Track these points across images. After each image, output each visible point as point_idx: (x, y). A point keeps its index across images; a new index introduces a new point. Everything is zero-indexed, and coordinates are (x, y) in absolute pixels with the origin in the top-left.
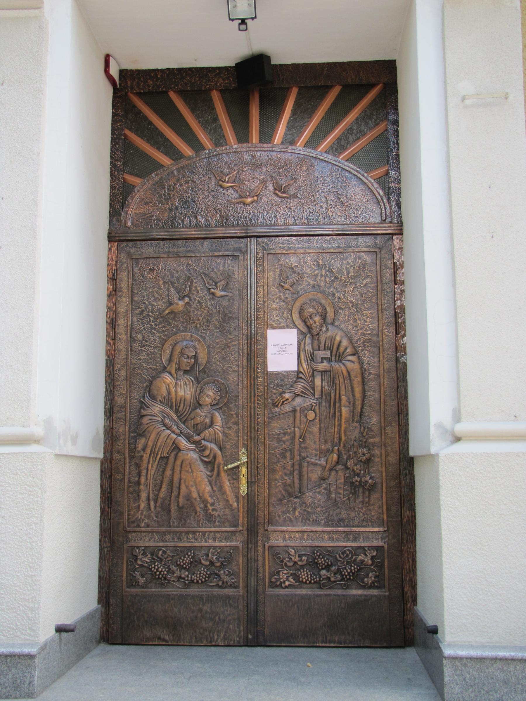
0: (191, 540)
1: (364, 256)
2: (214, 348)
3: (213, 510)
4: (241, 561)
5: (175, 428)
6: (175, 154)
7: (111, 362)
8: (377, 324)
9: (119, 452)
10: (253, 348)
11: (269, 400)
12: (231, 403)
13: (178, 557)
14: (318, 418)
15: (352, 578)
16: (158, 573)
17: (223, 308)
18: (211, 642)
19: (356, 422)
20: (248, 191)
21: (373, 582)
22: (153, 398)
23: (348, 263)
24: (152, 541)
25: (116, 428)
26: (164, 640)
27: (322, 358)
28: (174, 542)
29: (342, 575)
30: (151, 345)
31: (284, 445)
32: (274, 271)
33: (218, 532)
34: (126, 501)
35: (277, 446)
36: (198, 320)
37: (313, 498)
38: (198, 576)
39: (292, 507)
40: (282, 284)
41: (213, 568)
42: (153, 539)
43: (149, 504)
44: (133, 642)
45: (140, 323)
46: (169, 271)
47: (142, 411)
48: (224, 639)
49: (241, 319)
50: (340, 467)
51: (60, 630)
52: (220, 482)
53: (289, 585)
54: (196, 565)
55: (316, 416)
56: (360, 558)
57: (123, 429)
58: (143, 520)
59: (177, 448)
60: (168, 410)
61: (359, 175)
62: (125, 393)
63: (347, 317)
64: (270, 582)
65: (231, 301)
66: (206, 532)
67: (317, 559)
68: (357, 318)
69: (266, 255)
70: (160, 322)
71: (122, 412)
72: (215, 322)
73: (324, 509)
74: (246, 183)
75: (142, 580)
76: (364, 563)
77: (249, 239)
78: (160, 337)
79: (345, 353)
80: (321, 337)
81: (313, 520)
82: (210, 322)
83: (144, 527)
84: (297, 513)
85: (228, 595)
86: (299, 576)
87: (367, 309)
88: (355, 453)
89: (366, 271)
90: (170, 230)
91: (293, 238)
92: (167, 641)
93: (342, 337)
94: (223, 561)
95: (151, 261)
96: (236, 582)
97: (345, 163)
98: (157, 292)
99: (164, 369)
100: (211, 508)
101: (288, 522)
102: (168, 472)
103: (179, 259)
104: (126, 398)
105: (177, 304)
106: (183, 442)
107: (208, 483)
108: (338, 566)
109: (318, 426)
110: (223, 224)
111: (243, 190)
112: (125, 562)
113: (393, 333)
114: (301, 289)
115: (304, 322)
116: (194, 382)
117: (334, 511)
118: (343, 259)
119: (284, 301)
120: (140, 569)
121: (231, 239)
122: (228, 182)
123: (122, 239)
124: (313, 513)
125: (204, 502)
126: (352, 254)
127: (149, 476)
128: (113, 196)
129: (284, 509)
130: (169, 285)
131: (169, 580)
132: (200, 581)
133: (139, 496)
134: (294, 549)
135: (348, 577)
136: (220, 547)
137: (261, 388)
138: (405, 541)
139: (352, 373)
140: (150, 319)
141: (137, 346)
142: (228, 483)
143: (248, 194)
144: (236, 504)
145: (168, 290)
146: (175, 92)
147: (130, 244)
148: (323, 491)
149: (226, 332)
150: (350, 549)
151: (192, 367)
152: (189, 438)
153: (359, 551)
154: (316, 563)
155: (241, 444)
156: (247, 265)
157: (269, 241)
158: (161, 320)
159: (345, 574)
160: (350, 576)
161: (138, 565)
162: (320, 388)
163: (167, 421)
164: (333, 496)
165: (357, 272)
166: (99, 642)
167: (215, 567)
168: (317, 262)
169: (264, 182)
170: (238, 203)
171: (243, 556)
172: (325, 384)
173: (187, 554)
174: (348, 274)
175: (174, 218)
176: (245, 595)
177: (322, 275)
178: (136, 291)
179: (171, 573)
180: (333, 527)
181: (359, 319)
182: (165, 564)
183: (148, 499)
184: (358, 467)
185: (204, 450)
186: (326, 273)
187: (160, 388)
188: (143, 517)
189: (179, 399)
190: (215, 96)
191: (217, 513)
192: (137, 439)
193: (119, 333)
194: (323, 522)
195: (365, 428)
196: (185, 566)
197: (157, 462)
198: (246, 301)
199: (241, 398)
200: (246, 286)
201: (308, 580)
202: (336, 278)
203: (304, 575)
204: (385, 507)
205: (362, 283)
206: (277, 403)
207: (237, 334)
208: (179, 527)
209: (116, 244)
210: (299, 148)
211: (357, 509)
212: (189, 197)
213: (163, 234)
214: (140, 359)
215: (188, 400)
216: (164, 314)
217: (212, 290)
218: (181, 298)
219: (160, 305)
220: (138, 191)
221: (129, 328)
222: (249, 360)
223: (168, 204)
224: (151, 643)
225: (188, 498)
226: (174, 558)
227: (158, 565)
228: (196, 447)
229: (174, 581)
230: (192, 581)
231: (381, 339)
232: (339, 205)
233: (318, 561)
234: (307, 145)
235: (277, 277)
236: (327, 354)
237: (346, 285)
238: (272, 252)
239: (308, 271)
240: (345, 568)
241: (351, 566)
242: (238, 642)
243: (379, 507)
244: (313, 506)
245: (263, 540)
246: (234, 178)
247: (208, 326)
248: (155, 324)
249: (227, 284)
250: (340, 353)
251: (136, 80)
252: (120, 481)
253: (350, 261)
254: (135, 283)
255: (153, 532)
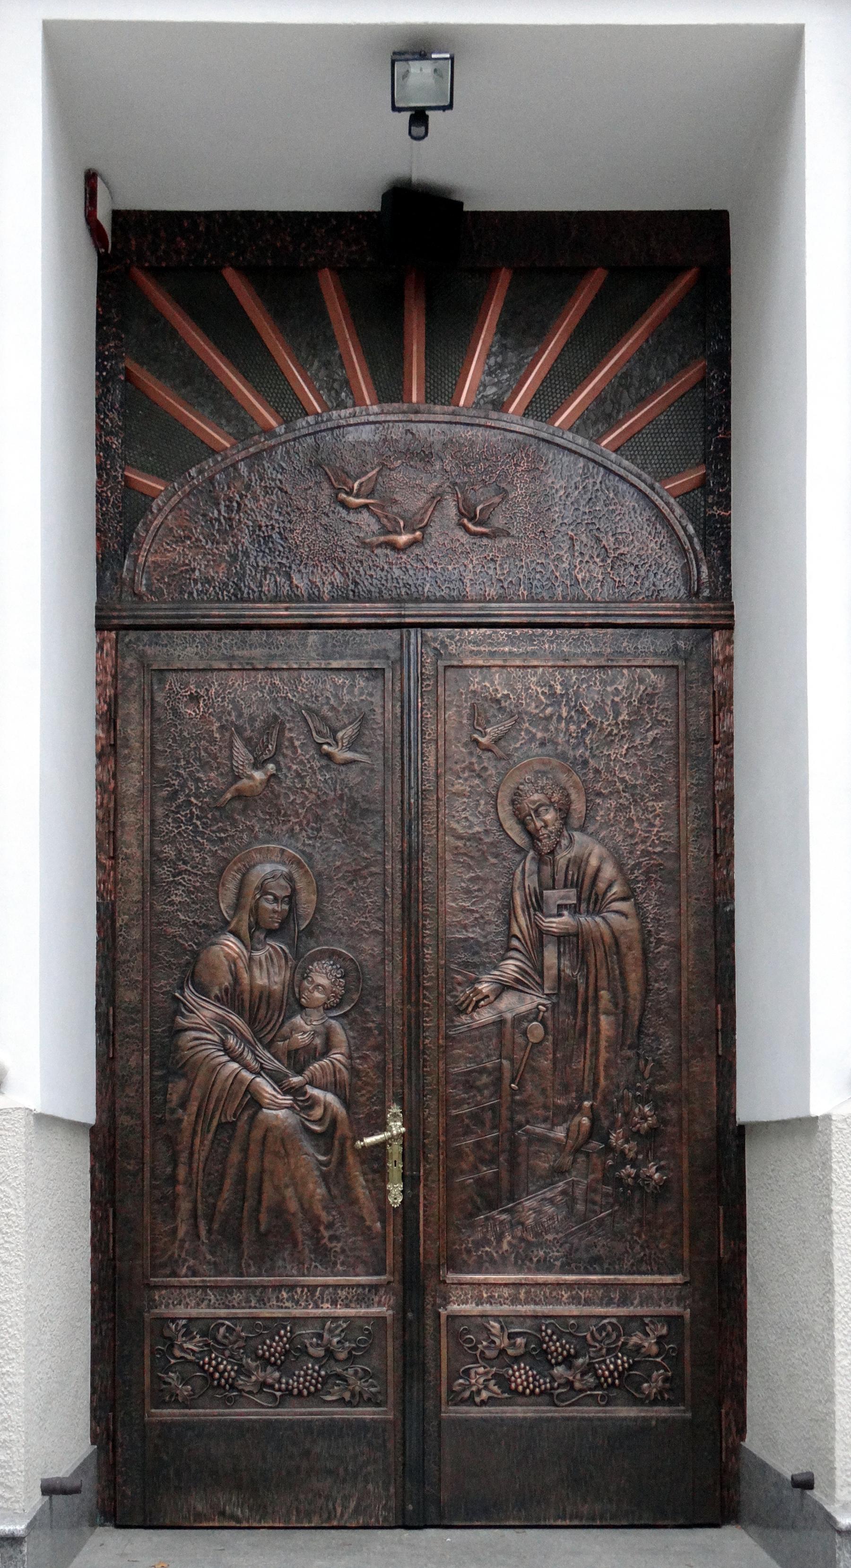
0: (287, 1304)
1: (652, 677)
2: (330, 879)
3: (332, 1238)
4: (390, 1349)
5: (249, 1057)
6: (242, 426)
7: (107, 907)
8: (676, 830)
9: (129, 1111)
10: (414, 881)
11: (449, 998)
12: (368, 1003)
13: (259, 1340)
14: (550, 1038)
15: (617, 1382)
16: (217, 1375)
17: (350, 789)
18: (329, 1519)
19: (630, 1047)
20: (402, 518)
21: (660, 1392)
22: (203, 990)
23: (617, 692)
24: (203, 1305)
25: (122, 1058)
26: (233, 1517)
27: (560, 907)
28: (250, 1307)
29: (598, 1377)
30: (195, 871)
31: (479, 1098)
32: (458, 706)
33: (342, 1287)
34: (147, 1218)
35: (464, 1099)
36: (297, 815)
37: (538, 1212)
38: (301, 1379)
39: (495, 1231)
40: (476, 736)
41: (332, 1362)
42: (206, 1302)
43: (196, 1226)
44: (168, 1522)
45: (170, 820)
46: (232, 701)
47: (179, 1019)
48: (356, 1512)
49: (388, 814)
50: (595, 1145)
51: (49, 1489)
52: (345, 1178)
53: (489, 1398)
54: (297, 1358)
55: (546, 1033)
56: (634, 1340)
57: (135, 1059)
58: (185, 1260)
59: (254, 1102)
60: (235, 1019)
61: (643, 486)
62: (140, 979)
63: (612, 815)
64: (450, 1391)
65: (367, 773)
66: (317, 1286)
67: (547, 1343)
68: (634, 818)
69: (441, 669)
70: (215, 819)
71: (134, 1021)
72: (332, 820)
73: (561, 1235)
74: (398, 497)
75: (185, 1390)
76: (643, 1350)
77: (405, 630)
78: (214, 854)
79: (609, 894)
80: (558, 857)
81: (539, 1261)
82: (322, 821)
83: (186, 1276)
84: (505, 1246)
85: (364, 1420)
86: (509, 1380)
87: (657, 797)
88: (626, 1115)
89: (655, 711)
90: (231, 605)
91: (501, 631)
92: (238, 1520)
93: (602, 860)
94: (354, 1349)
95: (193, 678)
96: (379, 1393)
97: (613, 456)
98: (206, 750)
99: (225, 926)
100: (326, 1234)
101: (487, 1264)
102: (235, 1157)
103: (253, 673)
104: (144, 990)
105: (251, 777)
106: (265, 1087)
107: (320, 1180)
108: (591, 1358)
109: (551, 1056)
110: (347, 594)
111: (390, 515)
112: (147, 1351)
113: (709, 852)
114: (516, 749)
115: (522, 822)
116: (290, 956)
117: (581, 1239)
118: (606, 682)
119: (479, 776)
120: (178, 1368)
121: (365, 631)
122: (357, 496)
123: (127, 622)
124: (540, 1245)
125: (315, 1222)
126: (625, 671)
127: (195, 1165)
128: (104, 520)
129: (479, 1236)
130: (232, 735)
131: (240, 1391)
132: (305, 1392)
133: (173, 1206)
134: (500, 1322)
135: (610, 1380)
136: (346, 1319)
137: (431, 969)
138: (724, 1305)
139: (623, 940)
140: (192, 813)
141: (164, 872)
142: (361, 1179)
143: (402, 524)
144: (378, 1224)
145: (231, 746)
146: (237, 268)
147: (146, 636)
148: (559, 1198)
149: (358, 845)
150: (614, 1320)
151: (284, 923)
152: (277, 1079)
153: (635, 1325)
154: (545, 1352)
155: (389, 1095)
156: (402, 691)
157: (448, 637)
158: (217, 814)
159: (603, 1375)
160: (614, 1379)
161: (175, 1358)
162: (555, 972)
163: (232, 1041)
164: (580, 1207)
165: (636, 713)
166: (93, 1525)
167: (337, 1361)
168: (551, 686)
169: (437, 499)
170: (380, 545)
171: (394, 1338)
172: (566, 962)
173: (278, 1334)
174: (616, 718)
175: (242, 578)
176: (400, 1423)
177: (560, 717)
178: (160, 747)
179: (243, 1374)
180: (580, 1273)
181: (638, 819)
182: (232, 1356)
183: (194, 1215)
184: (633, 1144)
185: (311, 1107)
186: (569, 713)
187: (216, 968)
188: (183, 1255)
189: (256, 993)
190: (327, 281)
191: (339, 1245)
192: (168, 1082)
193: (124, 843)
194: (558, 1263)
195: (647, 1061)
196: (273, 1359)
197: (210, 1136)
198: (398, 774)
199: (388, 992)
200: (399, 739)
201: (528, 1387)
202: (591, 725)
203: (520, 1375)
204: (686, 1232)
205: (645, 738)
206: (464, 1005)
207: (380, 850)
208: (260, 1275)
209: (113, 634)
210: (514, 419)
211: (629, 1237)
212: (273, 529)
213: (218, 613)
214: (172, 903)
215: (278, 996)
216: (222, 800)
217: (325, 747)
218: (258, 764)
219: (213, 778)
220: (160, 510)
221: (147, 831)
222: (406, 908)
223: (226, 543)
224: (205, 1524)
225: (279, 1211)
226: (252, 1343)
227: (216, 1357)
228: (295, 1100)
229: (250, 1392)
230: (288, 1392)
231: (683, 865)
232: (598, 556)
233: (548, 1347)
234: (528, 412)
235: (465, 721)
236: (570, 896)
237: (612, 741)
238: (455, 663)
239: (532, 709)
240: (604, 1361)
241: (617, 1357)
242: (385, 1519)
243: (675, 1233)
244: (539, 1230)
245: (435, 1301)
246: (371, 485)
247: (319, 830)
248: (203, 823)
249: (360, 734)
250: (596, 894)
251: (150, 237)
252: (135, 1175)
253: (620, 688)
254: (157, 727)
255: (204, 1288)
